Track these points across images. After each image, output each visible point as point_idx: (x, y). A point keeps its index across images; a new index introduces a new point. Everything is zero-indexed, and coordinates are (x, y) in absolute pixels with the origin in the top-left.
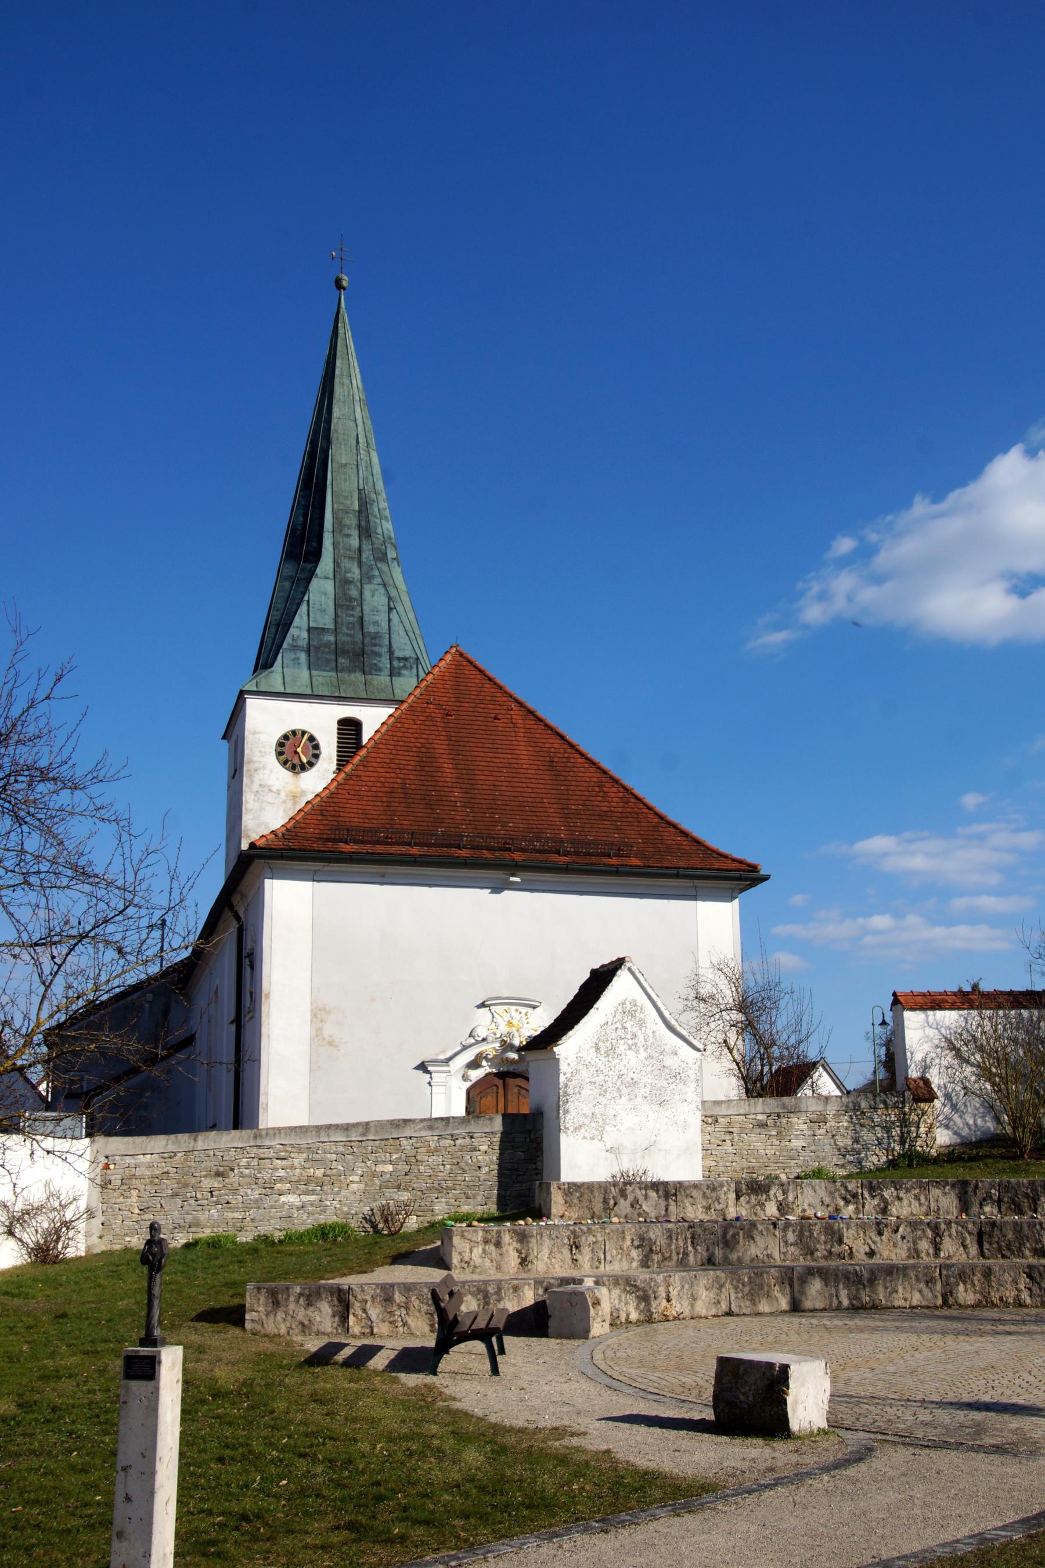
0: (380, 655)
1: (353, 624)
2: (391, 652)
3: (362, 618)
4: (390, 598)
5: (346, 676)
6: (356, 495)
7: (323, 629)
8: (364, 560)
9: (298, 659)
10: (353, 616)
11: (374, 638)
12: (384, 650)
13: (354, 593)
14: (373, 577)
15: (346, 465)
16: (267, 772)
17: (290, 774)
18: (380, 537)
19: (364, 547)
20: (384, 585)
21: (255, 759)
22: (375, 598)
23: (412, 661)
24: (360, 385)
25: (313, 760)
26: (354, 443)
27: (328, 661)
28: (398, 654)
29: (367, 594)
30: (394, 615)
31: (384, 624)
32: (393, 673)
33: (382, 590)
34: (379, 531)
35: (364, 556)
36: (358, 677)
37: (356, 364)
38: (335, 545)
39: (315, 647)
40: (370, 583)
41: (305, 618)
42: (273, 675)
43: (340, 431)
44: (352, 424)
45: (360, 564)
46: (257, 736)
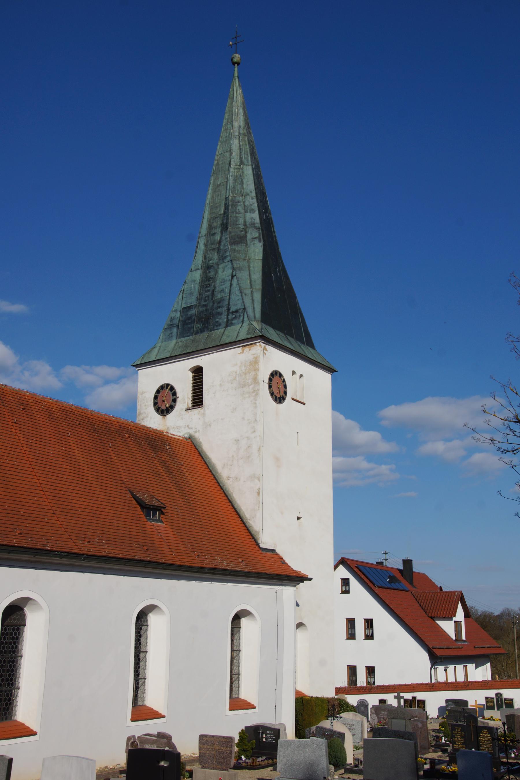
0: (222, 314)
1: (208, 297)
2: (229, 309)
3: (213, 290)
4: (233, 269)
6: (223, 203)
7: (189, 307)
8: (222, 247)
9: (172, 333)
10: (209, 291)
11: (219, 302)
12: (224, 310)
13: (212, 274)
14: (226, 257)
15: (220, 185)
16: (149, 419)
17: (161, 417)
18: (242, 226)
19: (223, 238)
20: (231, 261)
21: (142, 411)
22: (225, 272)
23: (240, 311)
24: (242, 124)
25: (173, 404)
26: (227, 166)
27: (190, 329)
28: (233, 309)
29: (220, 271)
30: (235, 282)
31: (227, 290)
32: (229, 324)
33: (230, 265)
34: (241, 221)
35: (222, 244)
36: (206, 334)
37: (241, 111)
38: (206, 245)
39: (182, 321)
40: (223, 262)
41: (180, 302)
42: (154, 349)
43: (221, 163)
44: (228, 154)
45: (219, 250)
46: (144, 395)
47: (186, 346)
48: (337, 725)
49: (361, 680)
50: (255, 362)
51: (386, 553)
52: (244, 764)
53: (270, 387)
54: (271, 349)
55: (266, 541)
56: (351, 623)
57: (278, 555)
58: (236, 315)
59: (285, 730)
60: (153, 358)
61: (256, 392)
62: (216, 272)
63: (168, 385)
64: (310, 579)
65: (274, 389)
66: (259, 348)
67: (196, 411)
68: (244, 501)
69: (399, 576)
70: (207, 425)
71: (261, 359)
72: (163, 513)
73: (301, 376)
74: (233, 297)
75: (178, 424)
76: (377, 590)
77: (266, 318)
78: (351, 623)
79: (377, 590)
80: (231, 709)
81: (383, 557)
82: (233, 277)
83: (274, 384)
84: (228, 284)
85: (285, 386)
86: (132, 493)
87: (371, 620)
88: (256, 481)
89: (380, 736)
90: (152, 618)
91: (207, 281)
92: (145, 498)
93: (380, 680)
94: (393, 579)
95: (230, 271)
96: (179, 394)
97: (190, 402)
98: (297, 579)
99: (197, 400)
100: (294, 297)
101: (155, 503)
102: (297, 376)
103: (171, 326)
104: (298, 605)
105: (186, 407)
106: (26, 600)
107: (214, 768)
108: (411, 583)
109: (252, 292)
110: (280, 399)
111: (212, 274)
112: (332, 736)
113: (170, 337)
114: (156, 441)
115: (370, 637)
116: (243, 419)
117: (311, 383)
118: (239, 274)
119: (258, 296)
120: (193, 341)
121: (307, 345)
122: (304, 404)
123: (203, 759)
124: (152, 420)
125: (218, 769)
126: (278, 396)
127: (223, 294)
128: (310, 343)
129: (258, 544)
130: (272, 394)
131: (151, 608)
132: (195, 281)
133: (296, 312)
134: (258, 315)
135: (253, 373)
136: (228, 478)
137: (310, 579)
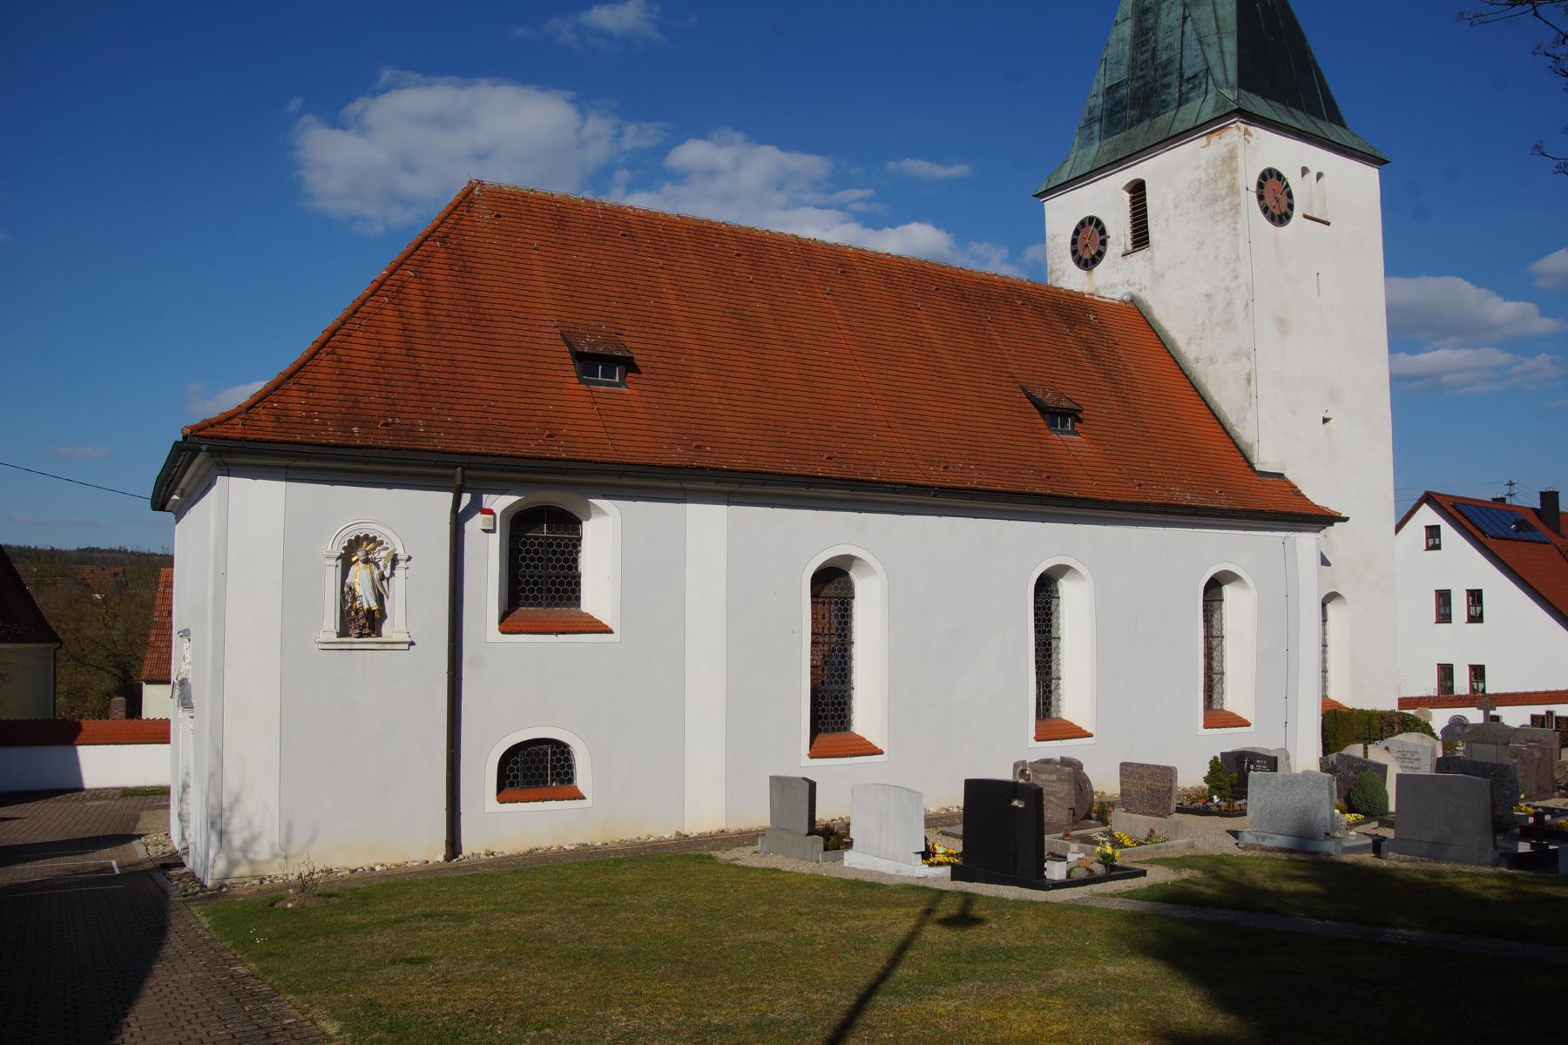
1: (1146, 61)
2: (1181, 75)
5: (1133, 131)
12: (1173, 79)
13: (1150, 22)
28: (1188, 73)
29: (1163, 14)
30: (1189, 26)
31: (1177, 44)
32: (1183, 100)
36: (1146, 124)
47: (1116, 150)
48: (1376, 753)
49: (1462, 685)
50: (1231, 156)
51: (1511, 484)
52: (1214, 808)
53: (1260, 198)
54: (1258, 133)
55: (1265, 459)
56: (1444, 597)
57: (1287, 481)
58: (1193, 83)
59: (1288, 758)
60: (1065, 179)
61: (1235, 209)
62: (1157, 17)
63: (1091, 219)
64: (1346, 519)
65: (1269, 201)
66: (1235, 132)
67: (1139, 255)
68: (1225, 395)
69: (1533, 520)
70: (1158, 276)
71: (1240, 152)
72: (1079, 420)
73: (1319, 176)
74: (1186, 53)
75: (1111, 280)
76: (1489, 542)
77: (1248, 79)
78: (1444, 597)
79: (1489, 542)
80: (1208, 725)
81: (1506, 490)
82: (1185, 19)
83: (1267, 192)
84: (1178, 33)
85: (1290, 195)
86: (1025, 391)
87: (1479, 592)
88: (1244, 360)
89: (1448, 770)
90: (1065, 587)
91: (1143, 35)
92: (1049, 399)
93: (1492, 686)
94: (1522, 525)
95: (1180, 10)
96: (1110, 231)
97: (1129, 242)
98: (1322, 519)
99: (1140, 237)
100: (1302, 39)
101: (1065, 404)
102: (1312, 176)
103: (1090, 122)
104: (1325, 562)
105: (1122, 251)
106: (850, 559)
107: (1143, 813)
108: (1557, 530)
109: (1220, 39)
110: (1279, 216)
111: (1150, 22)
112: (1364, 769)
113: (1089, 140)
114: (1074, 309)
115: (1476, 618)
116: (1217, 257)
117: (1343, 189)
118: (1196, 13)
119: (1231, 45)
120: (1126, 140)
121: (1331, 121)
122: (1328, 224)
123: (1127, 800)
124: (1069, 277)
125: (1151, 814)
126: (1277, 213)
127: (1171, 53)
128: (1335, 117)
129: (1251, 466)
130: (1265, 210)
131: (1062, 570)
132: (1123, 40)
133: (1306, 63)
134: (1232, 75)
135: (1228, 177)
136: (1197, 360)
137: (1346, 519)
